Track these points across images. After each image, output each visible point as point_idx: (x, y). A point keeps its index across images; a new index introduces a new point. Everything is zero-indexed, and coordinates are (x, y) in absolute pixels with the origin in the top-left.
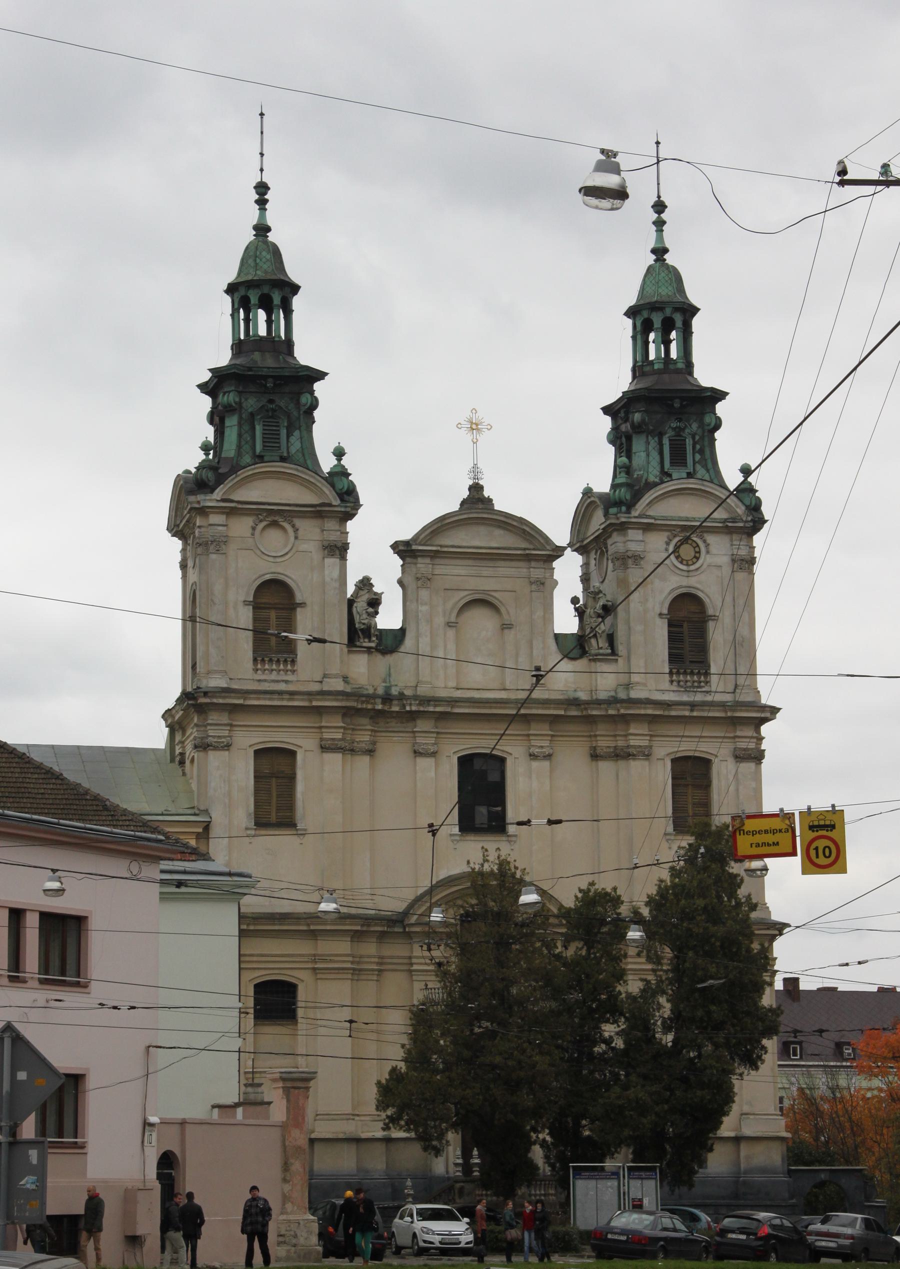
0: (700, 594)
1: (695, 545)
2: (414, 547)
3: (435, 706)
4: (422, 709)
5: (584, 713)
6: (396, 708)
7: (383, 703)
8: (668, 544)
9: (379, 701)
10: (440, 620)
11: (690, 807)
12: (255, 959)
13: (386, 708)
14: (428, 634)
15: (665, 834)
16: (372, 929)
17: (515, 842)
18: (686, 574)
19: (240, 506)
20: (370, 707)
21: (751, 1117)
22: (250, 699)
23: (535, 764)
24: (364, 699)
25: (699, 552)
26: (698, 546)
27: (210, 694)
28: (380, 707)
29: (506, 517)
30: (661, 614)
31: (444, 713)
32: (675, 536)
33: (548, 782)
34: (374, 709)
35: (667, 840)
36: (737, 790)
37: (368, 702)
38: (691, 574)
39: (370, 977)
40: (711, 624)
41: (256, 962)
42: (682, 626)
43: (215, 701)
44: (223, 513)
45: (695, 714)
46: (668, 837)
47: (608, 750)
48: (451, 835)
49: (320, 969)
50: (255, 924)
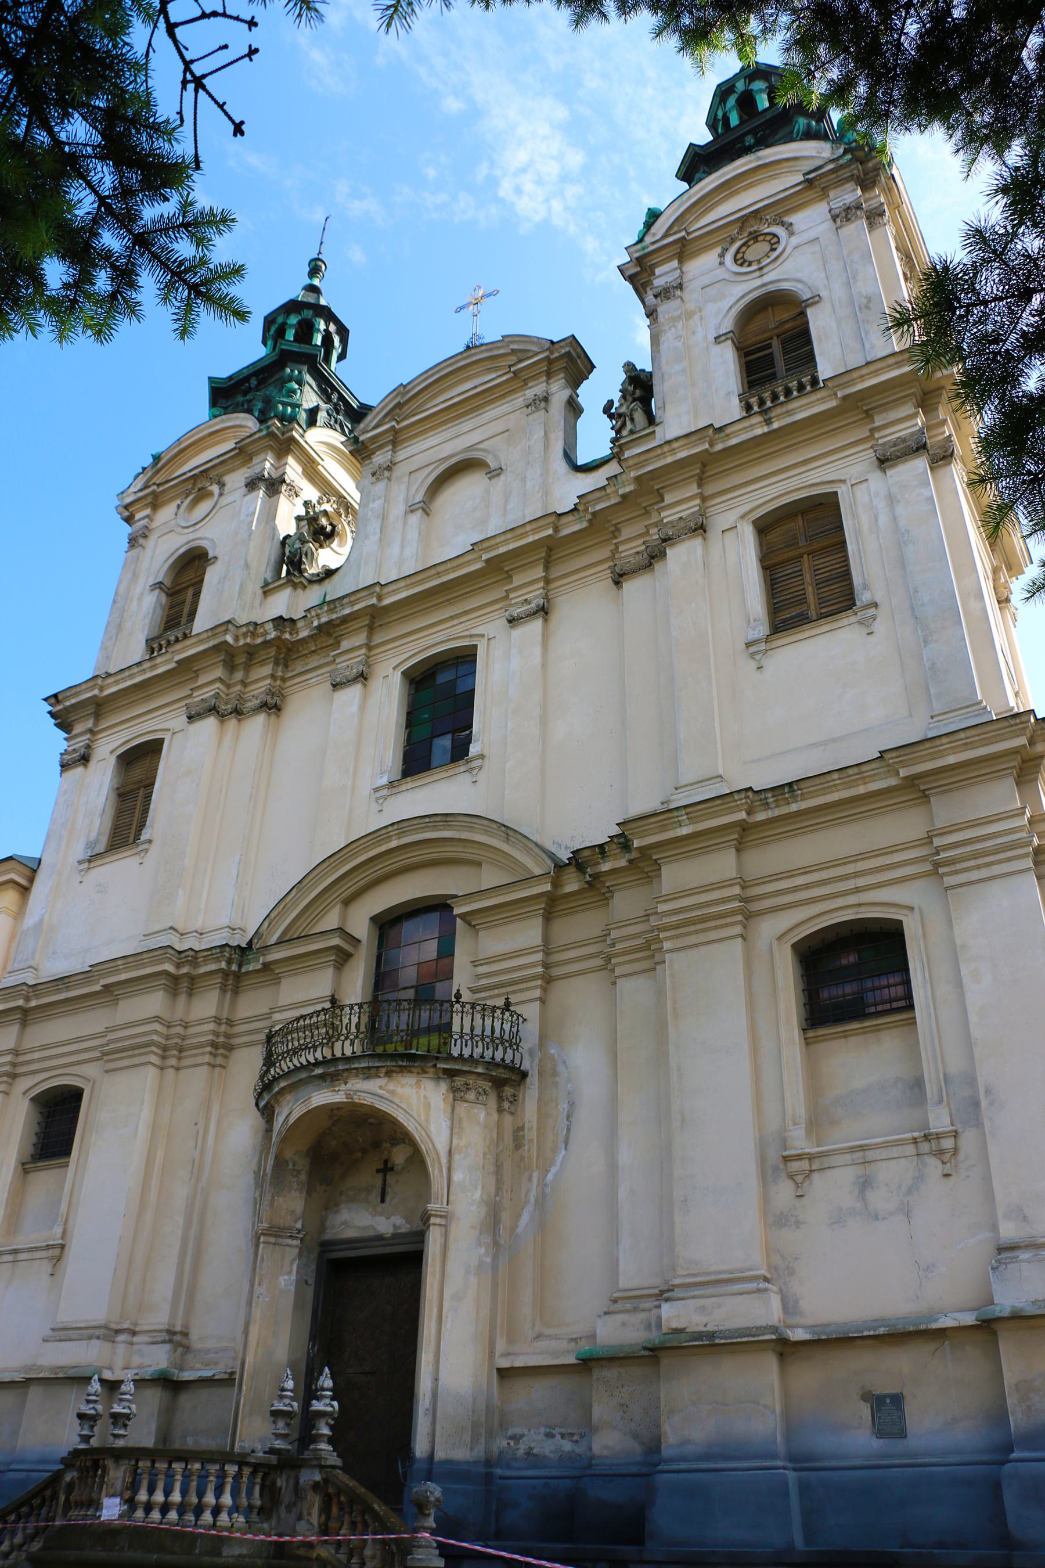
0: (785, 285)
1: (768, 238)
2: (361, 438)
3: (352, 604)
4: (334, 616)
5: (589, 516)
6: (304, 634)
7: (276, 628)
8: (722, 255)
9: (269, 626)
10: (398, 509)
11: (810, 590)
12: (37, 1055)
13: (287, 636)
14: (378, 531)
15: (748, 645)
16: (202, 970)
17: (480, 768)
18: (757, 274)
19: (161, 489)
20: (259, 640)
21: (1024, 1255)
22: (109, 686)
23: (518, 633)
24: (244, 629)
25: (778, 242)
26: (775, 235)
27: (60, 697)
28: (273, 635)
29: (487, 350)
30: (718, 339)
31: (375, 614)
32: (733, 241)
33: (537, 651)
34: (266, 644)
35: (752, 655)
36: (895, 519)
37: (254, 635)
38: (765, 270)
39: (199, 1060)
40: (809, 312)
41: (39, 1060)
42: (769, 346)
43: (67, 704)
44: (146, 506)
45: (776, 425)
46: (752, 649)
47: (638, 558)
48: (377, 790)
49: (115, 1054)
50: (37, 997)
